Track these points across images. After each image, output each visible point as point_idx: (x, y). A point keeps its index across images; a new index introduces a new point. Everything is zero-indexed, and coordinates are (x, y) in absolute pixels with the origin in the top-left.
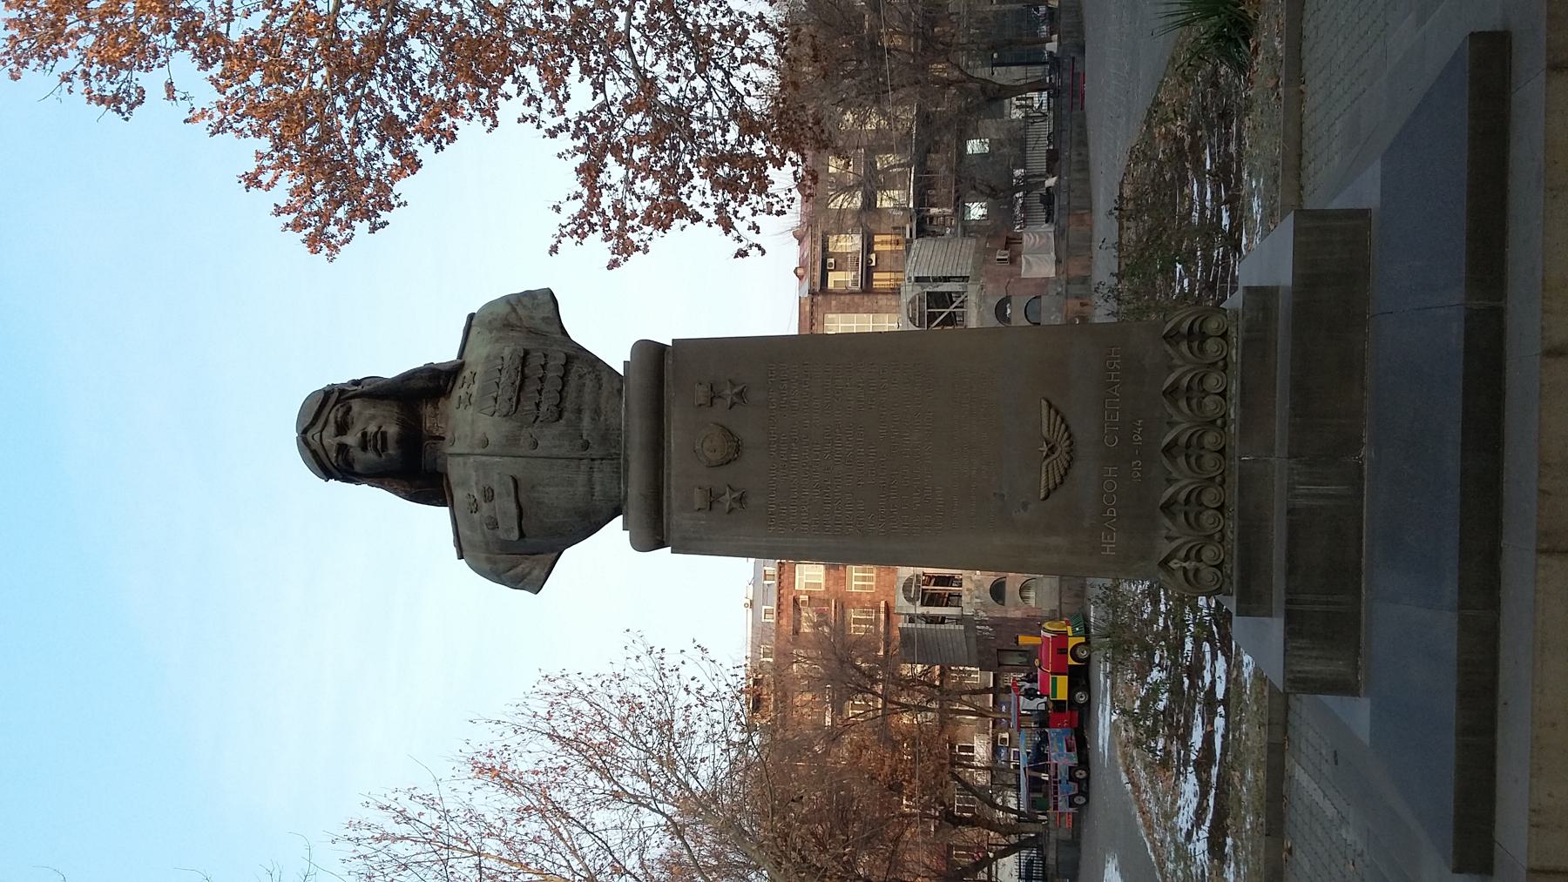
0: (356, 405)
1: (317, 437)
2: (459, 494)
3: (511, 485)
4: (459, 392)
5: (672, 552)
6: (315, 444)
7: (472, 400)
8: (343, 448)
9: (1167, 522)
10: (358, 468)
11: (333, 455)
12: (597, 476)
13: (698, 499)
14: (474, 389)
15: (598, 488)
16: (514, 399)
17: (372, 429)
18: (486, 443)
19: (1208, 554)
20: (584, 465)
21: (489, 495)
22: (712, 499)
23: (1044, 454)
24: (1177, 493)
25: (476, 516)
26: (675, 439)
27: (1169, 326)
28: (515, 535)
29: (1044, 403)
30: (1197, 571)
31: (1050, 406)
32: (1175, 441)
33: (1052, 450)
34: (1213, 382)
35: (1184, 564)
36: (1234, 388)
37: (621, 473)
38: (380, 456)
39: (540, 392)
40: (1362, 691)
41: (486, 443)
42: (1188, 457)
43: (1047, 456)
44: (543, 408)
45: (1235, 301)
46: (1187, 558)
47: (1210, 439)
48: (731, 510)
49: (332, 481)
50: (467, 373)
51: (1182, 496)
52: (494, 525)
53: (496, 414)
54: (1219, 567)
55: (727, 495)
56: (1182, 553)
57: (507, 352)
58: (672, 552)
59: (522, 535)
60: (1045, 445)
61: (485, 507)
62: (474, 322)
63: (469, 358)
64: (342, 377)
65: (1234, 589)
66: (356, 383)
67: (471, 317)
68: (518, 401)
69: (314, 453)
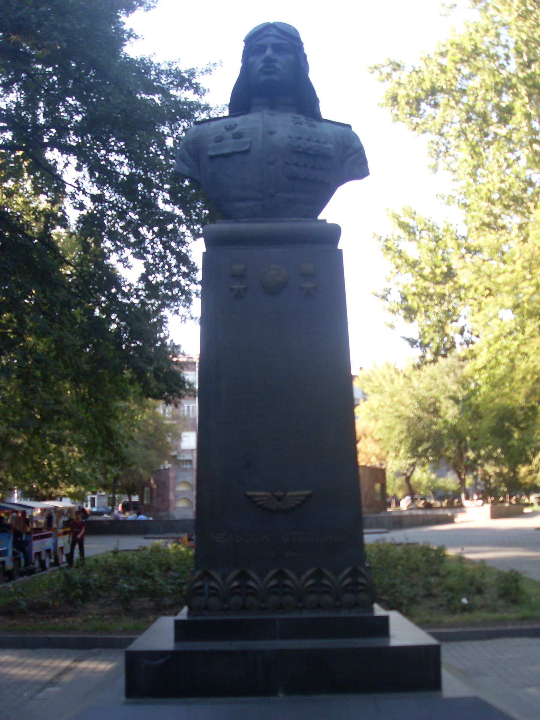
0: (291, 57)
1: (270, 33)
2: (238, 120)
4: (302, 118)
5: (203, 253)
6: (265, 33)
7: (298, 126)
8: (262, 49)
9: (233, 575)
10: (252, 59)
11: (260, 42)
13: (238, 268)
14: (305, 127)
15: (242, 204)
16: (300, 150)
17: (278, 65)
18: (271, 133)
19: (214, 601)
21: (238, 136)
22: (239, 277)
23: (276, 494)
24: (253, 580)
25: (223, 130)
27: (362, 570)
28: (211, 153)
29: (307, 492)
30: (202, 594)
31: (308, 497)
32: (287, 577)
33: (279, 499)
34: (327, 599)
35: (206, 587)
37: (253, 216)
38: (260, 70)
39: (305, 166)
40: (130, 700)
41: (271, 133)
42: (276, 586)
43: (275, 496)
44: (295, 168)
45: (379, 611)
46: (211, 588)
47: (289, 599)
48: (232, 290)
49: (243, 44)
50: (315, 123)
51: (251, 583)
52: (219, 139)
53: (289, 139)
55: (241, 287)
56: (213, 584)
57: (330, 146)
58: (203, 253)
59: (212, 158)
60: (282, 494)
61: (229, 134)
62: (346, 128)
63: (324, 125)
64: (308, 49)
65: (192, 618)
66: (305, 56)
67: (349, 126)
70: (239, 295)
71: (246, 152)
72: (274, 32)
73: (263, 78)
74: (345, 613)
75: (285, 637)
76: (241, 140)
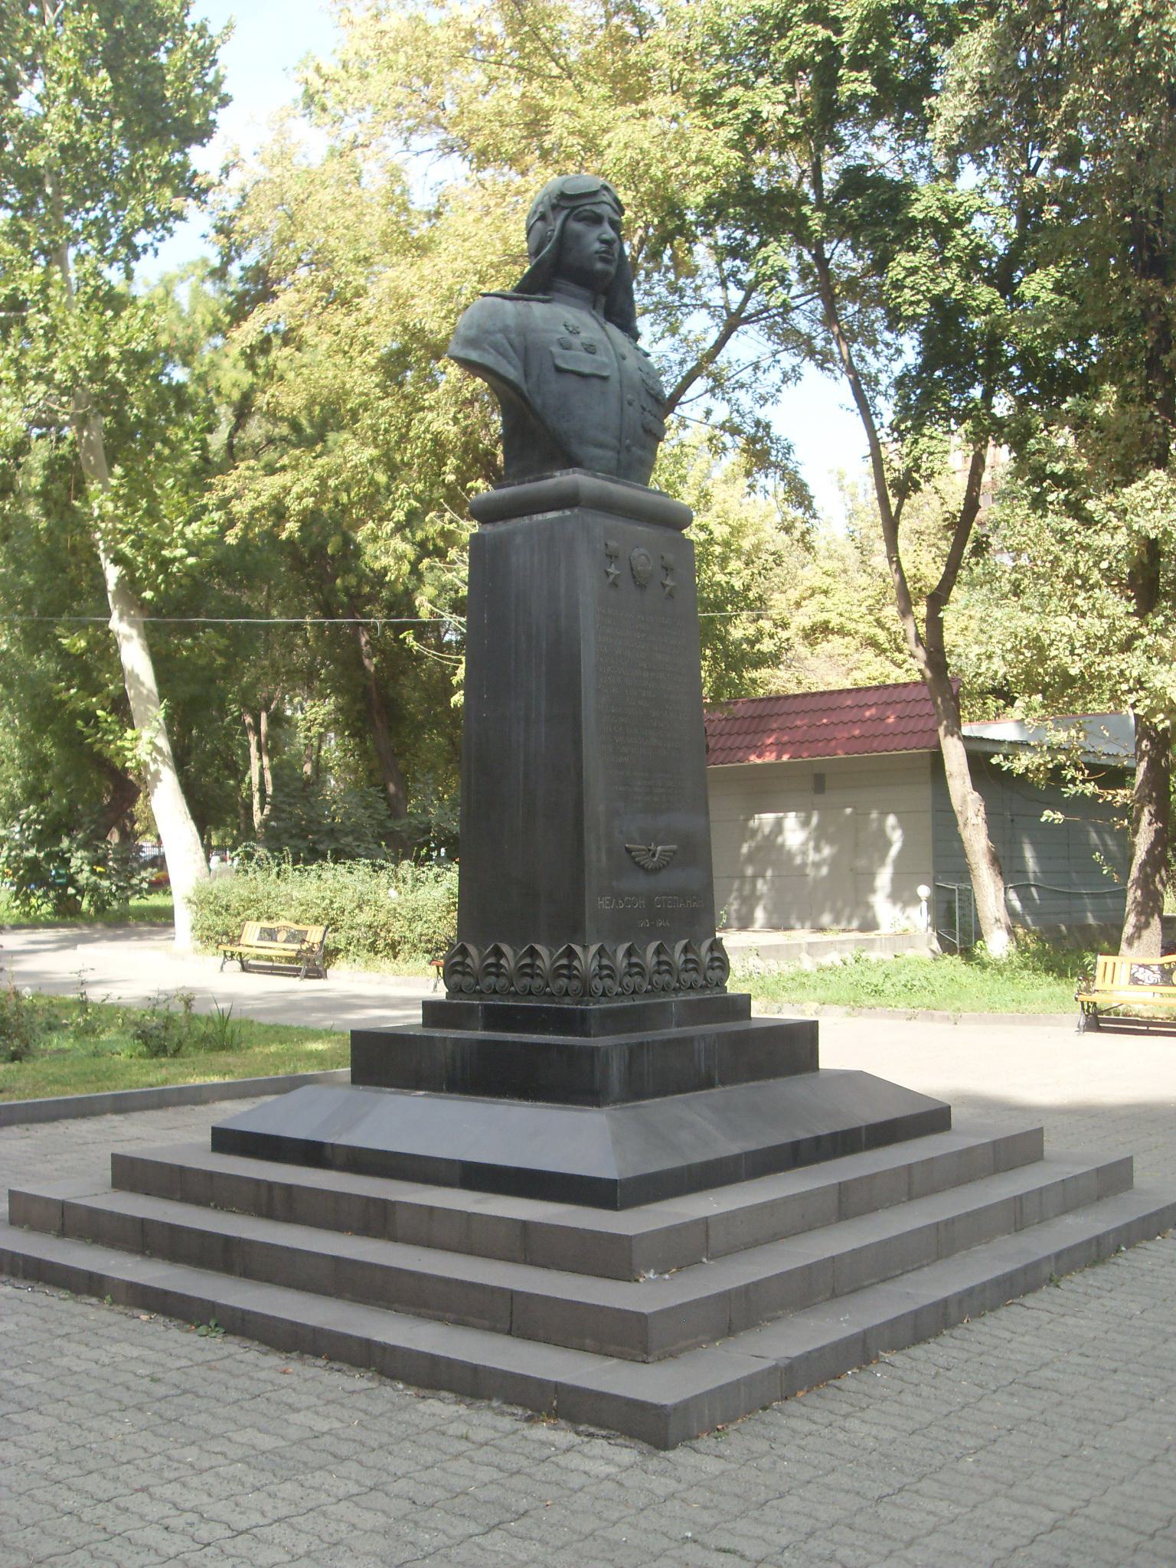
3: (605, 374)
11: (595, 208)
12: (610, 454)
15: (598, 452)
18: (624, 358)
20: (614, 442)
22: (612, 557)
26: (642, 530)
29: (675, 847)
31: (674, 852)
36: (693, 996)
38: (597, 252)
48: (607, 574)
54: (604, 995)
59: (559, 370)
68: (652, 396)
69: (595, 193)
70: (614, 584)
71: (605, 379)
72: (607, 198)
73: (599, 266)
74: (708, 994)
75: (678, 1025)
76: (597, 357)
